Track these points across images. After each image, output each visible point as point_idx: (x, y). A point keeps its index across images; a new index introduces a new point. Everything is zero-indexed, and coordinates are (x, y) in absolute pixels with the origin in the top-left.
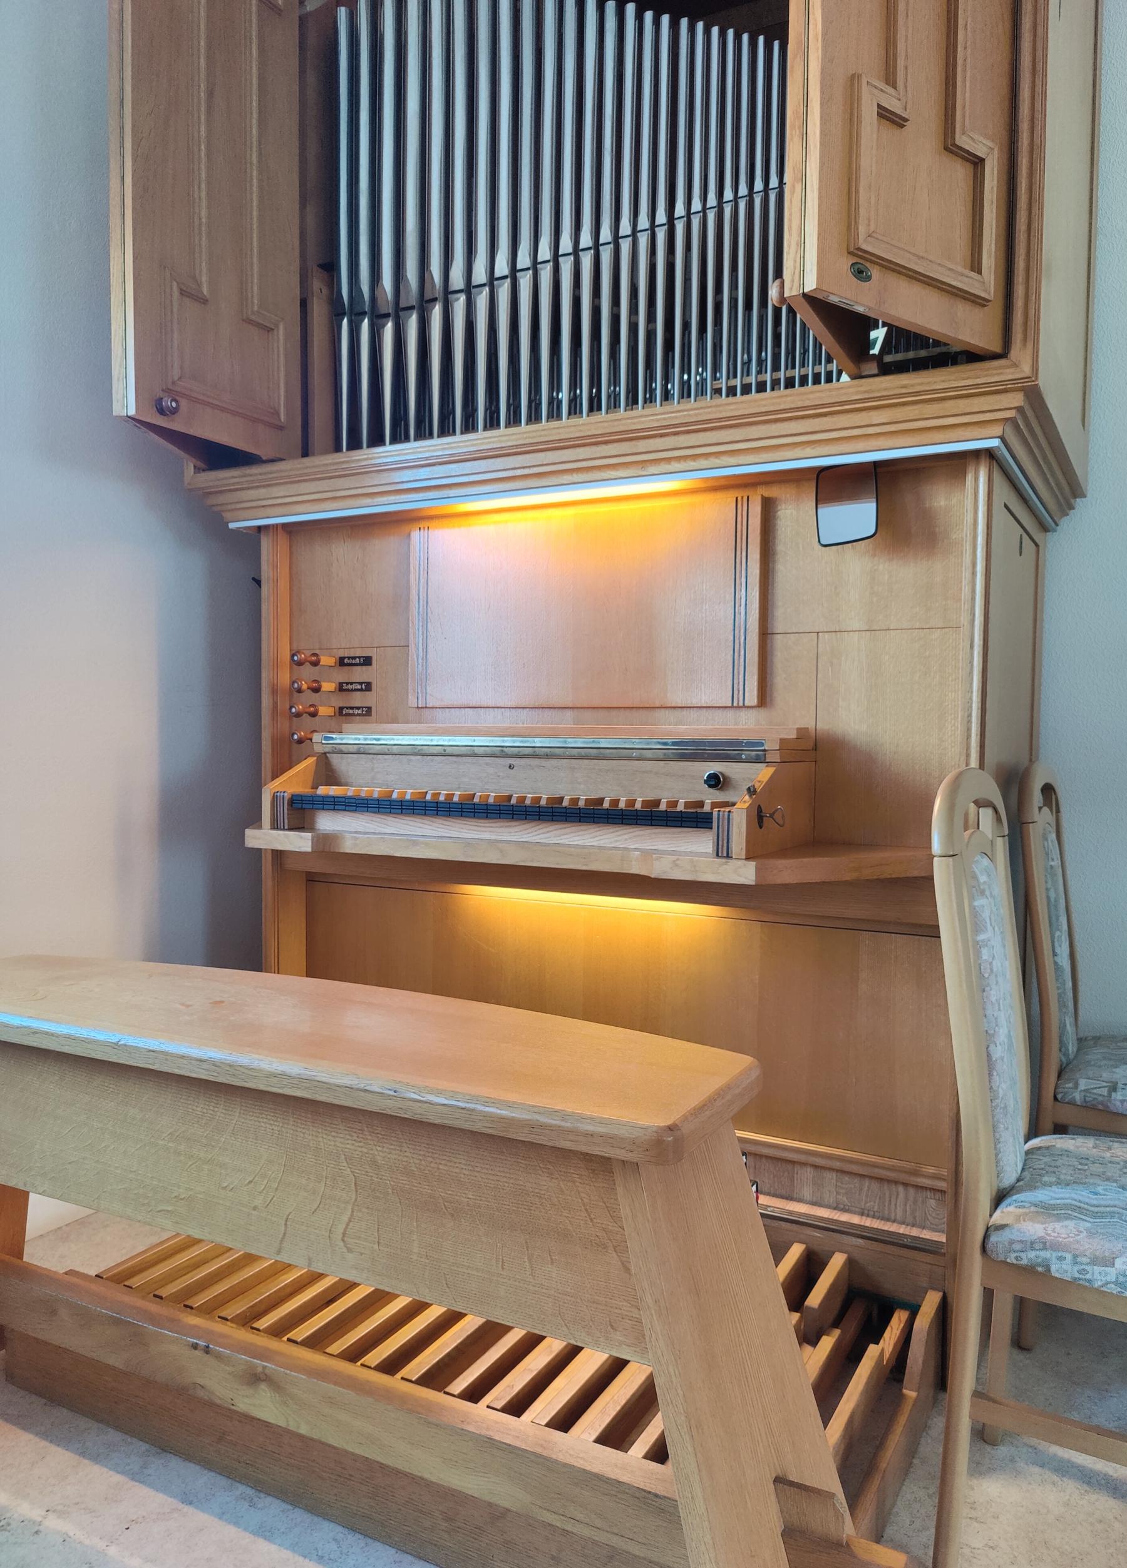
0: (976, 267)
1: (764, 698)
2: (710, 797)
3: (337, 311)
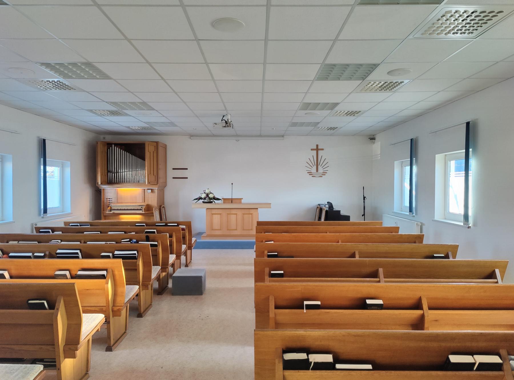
0: (155, 181)
1: (144, 202)
2: (141, 208)
3: (108, 172)
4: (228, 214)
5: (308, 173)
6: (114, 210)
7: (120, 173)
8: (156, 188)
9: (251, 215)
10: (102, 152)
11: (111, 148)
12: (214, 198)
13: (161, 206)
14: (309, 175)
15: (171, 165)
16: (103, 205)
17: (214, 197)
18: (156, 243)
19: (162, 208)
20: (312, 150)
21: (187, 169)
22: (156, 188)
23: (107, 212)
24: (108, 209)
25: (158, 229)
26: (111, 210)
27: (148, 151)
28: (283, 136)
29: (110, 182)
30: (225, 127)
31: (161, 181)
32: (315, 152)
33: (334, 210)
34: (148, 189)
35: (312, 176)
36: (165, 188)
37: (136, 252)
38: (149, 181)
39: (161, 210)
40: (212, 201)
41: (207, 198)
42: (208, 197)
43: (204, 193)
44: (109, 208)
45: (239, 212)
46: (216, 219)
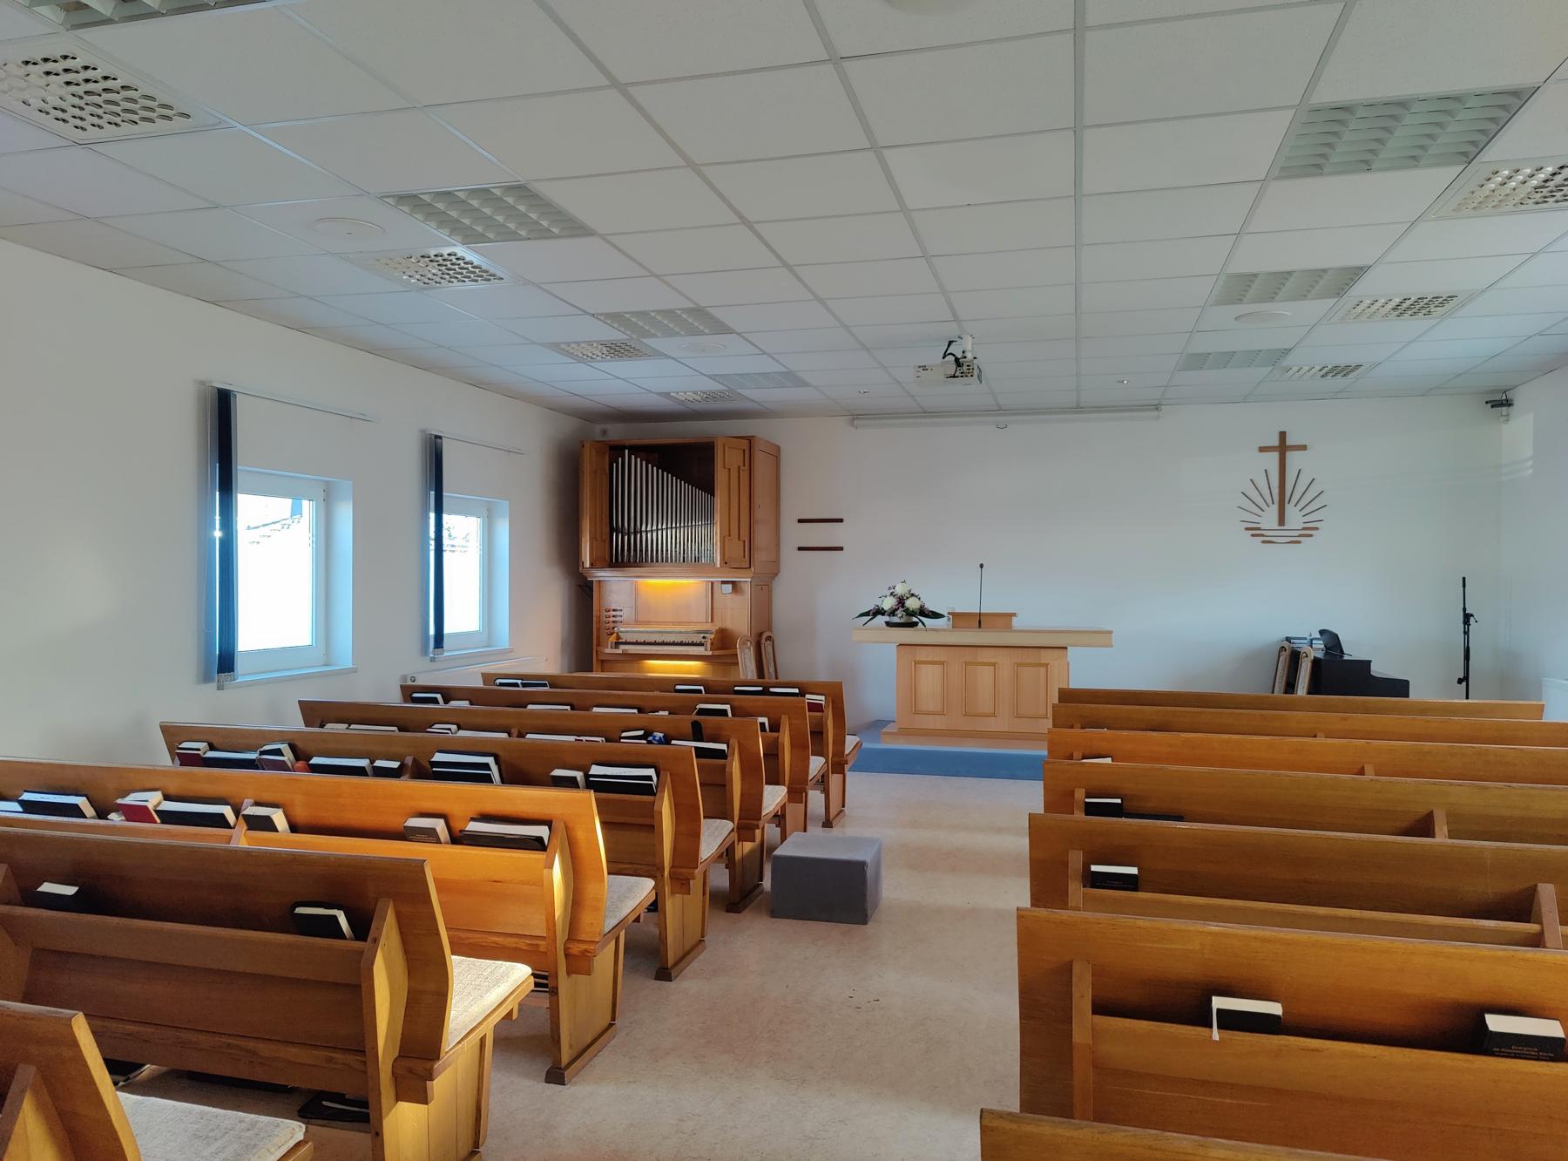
2: (703, 641)
3: (612, 530)
4: (967, 664)
5: (1247, 529)
6: (626, 643)
7: (644, 535)
8: (745, 579)
9: (1043, 670)
10: (596, 472)
11: (620, 459)
12: (923, 612)
13: (761, 634)
14: (1252, 535)
15: (792, 507)
16: (598, 629)
17: (922, 607)
18: (723, 747)
19: (763, 640)
20: (1262, 449)
21: (841, 520)
22: (745, 579)
23: (608, 650)
24: (611, 639)
25: (736, 704)
26: (617, 644)
27: (724, 467)
28: (1157, 407)
29: (617, 561)
30: (954, 377)
31: (761, 557)
32: (1275, 456)
33: (1346, 657)
34: (723, 582)
35: (1263, 542)
36: (776, 578)
37: (651, 772)
38: (726, 558)
39: (763, 646)
40: (915, 619)
41: (901, 609)
42: (903, 606)
43: (891, 594)
44: (613, 639)
45: (1005, 660)
46: (930, 678)
